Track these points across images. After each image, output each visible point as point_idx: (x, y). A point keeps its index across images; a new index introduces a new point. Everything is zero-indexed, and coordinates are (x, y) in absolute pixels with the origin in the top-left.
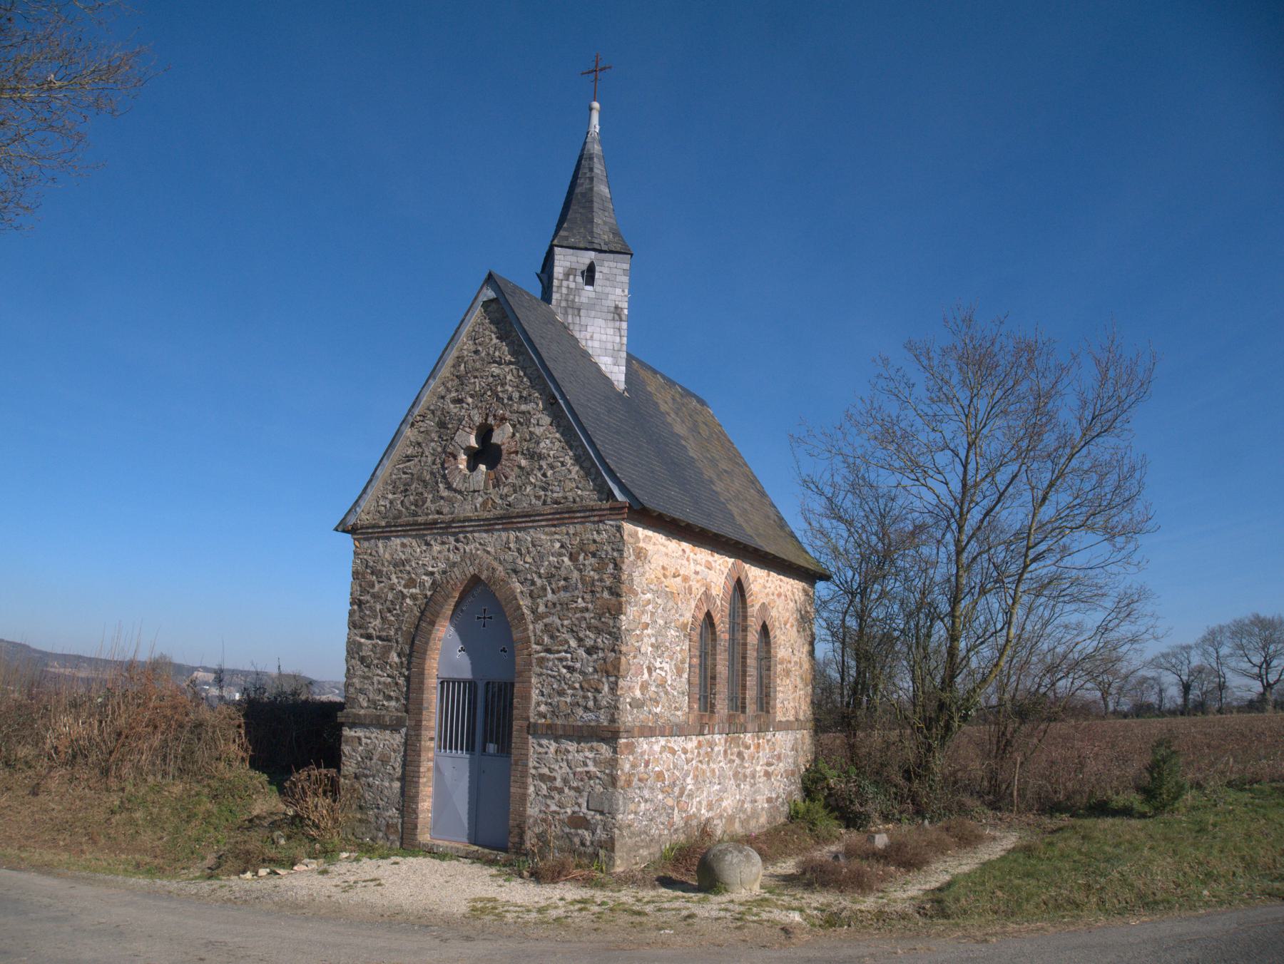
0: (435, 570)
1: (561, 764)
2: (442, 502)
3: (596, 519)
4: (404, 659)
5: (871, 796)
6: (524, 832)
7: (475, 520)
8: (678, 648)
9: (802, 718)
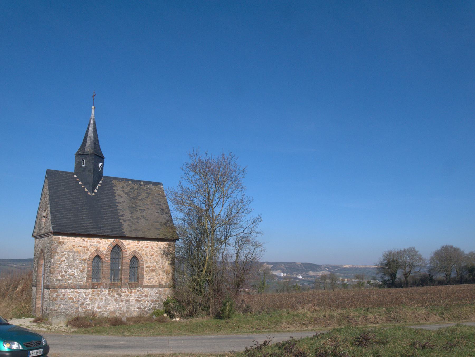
8: (81, 266)
9: (163, 283)
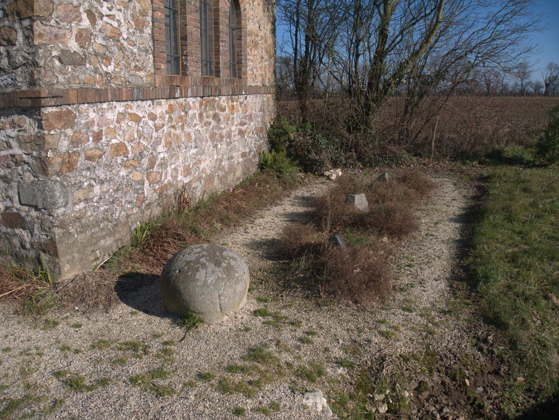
5: (324, 147)
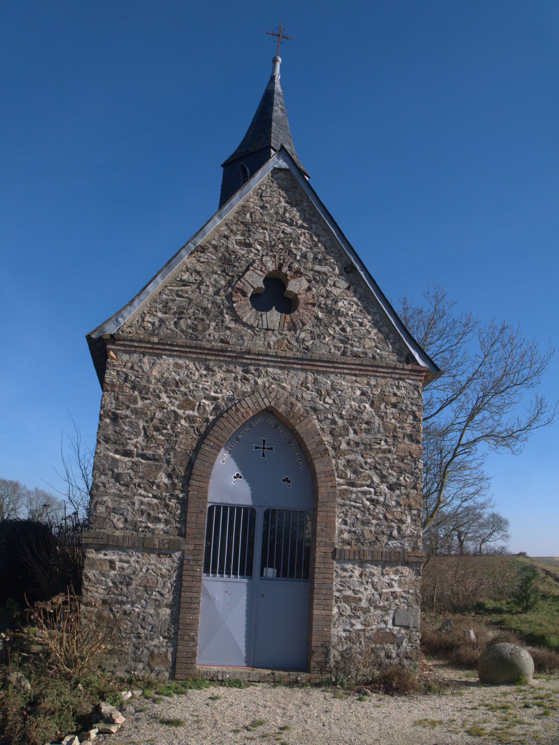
0: (220, 395)
1: (366, 586)
2: (228, 332)
3: (397, 376)
4: (176, 481)
6: (329, 651)
7: (272, 356)
